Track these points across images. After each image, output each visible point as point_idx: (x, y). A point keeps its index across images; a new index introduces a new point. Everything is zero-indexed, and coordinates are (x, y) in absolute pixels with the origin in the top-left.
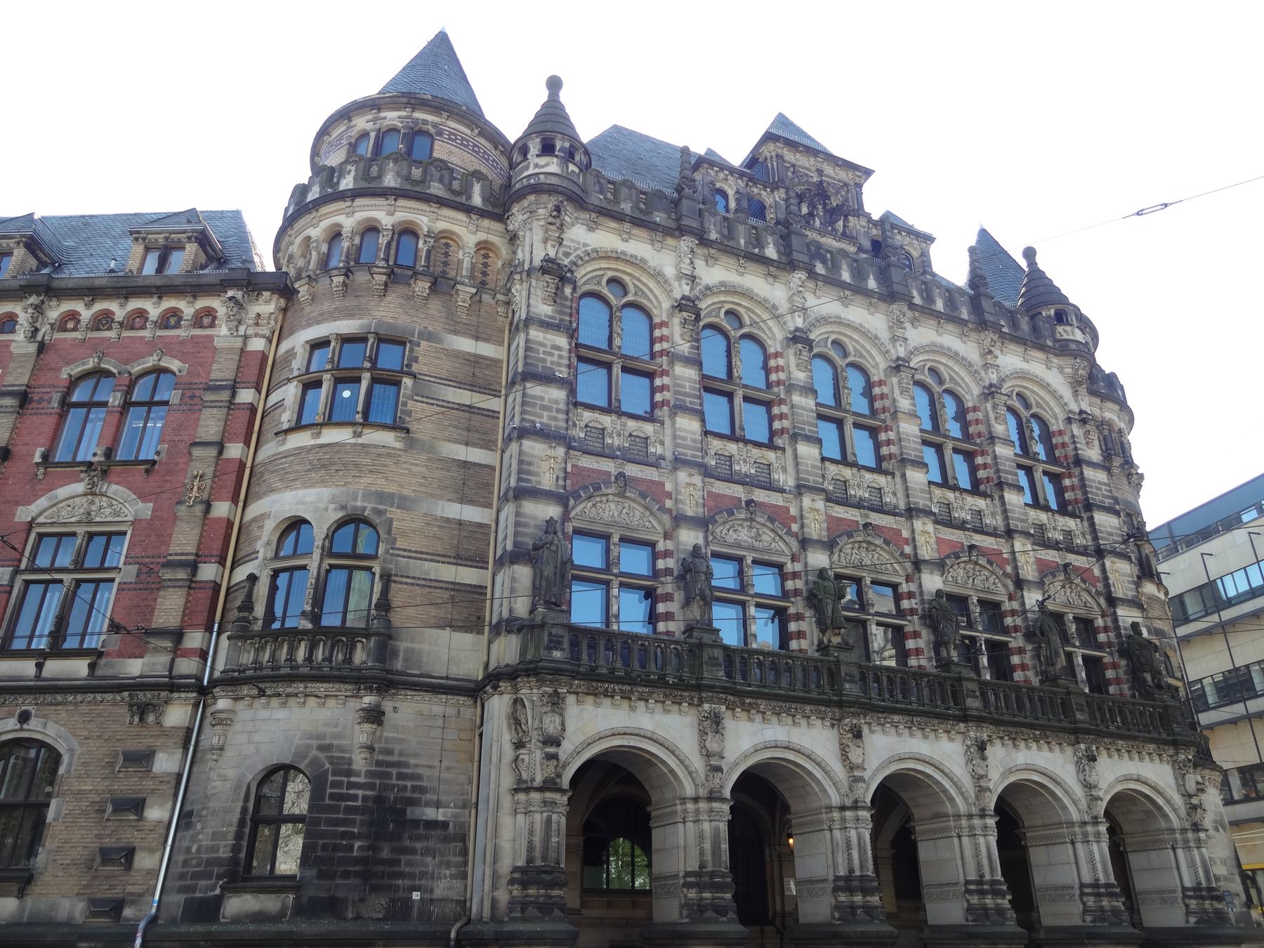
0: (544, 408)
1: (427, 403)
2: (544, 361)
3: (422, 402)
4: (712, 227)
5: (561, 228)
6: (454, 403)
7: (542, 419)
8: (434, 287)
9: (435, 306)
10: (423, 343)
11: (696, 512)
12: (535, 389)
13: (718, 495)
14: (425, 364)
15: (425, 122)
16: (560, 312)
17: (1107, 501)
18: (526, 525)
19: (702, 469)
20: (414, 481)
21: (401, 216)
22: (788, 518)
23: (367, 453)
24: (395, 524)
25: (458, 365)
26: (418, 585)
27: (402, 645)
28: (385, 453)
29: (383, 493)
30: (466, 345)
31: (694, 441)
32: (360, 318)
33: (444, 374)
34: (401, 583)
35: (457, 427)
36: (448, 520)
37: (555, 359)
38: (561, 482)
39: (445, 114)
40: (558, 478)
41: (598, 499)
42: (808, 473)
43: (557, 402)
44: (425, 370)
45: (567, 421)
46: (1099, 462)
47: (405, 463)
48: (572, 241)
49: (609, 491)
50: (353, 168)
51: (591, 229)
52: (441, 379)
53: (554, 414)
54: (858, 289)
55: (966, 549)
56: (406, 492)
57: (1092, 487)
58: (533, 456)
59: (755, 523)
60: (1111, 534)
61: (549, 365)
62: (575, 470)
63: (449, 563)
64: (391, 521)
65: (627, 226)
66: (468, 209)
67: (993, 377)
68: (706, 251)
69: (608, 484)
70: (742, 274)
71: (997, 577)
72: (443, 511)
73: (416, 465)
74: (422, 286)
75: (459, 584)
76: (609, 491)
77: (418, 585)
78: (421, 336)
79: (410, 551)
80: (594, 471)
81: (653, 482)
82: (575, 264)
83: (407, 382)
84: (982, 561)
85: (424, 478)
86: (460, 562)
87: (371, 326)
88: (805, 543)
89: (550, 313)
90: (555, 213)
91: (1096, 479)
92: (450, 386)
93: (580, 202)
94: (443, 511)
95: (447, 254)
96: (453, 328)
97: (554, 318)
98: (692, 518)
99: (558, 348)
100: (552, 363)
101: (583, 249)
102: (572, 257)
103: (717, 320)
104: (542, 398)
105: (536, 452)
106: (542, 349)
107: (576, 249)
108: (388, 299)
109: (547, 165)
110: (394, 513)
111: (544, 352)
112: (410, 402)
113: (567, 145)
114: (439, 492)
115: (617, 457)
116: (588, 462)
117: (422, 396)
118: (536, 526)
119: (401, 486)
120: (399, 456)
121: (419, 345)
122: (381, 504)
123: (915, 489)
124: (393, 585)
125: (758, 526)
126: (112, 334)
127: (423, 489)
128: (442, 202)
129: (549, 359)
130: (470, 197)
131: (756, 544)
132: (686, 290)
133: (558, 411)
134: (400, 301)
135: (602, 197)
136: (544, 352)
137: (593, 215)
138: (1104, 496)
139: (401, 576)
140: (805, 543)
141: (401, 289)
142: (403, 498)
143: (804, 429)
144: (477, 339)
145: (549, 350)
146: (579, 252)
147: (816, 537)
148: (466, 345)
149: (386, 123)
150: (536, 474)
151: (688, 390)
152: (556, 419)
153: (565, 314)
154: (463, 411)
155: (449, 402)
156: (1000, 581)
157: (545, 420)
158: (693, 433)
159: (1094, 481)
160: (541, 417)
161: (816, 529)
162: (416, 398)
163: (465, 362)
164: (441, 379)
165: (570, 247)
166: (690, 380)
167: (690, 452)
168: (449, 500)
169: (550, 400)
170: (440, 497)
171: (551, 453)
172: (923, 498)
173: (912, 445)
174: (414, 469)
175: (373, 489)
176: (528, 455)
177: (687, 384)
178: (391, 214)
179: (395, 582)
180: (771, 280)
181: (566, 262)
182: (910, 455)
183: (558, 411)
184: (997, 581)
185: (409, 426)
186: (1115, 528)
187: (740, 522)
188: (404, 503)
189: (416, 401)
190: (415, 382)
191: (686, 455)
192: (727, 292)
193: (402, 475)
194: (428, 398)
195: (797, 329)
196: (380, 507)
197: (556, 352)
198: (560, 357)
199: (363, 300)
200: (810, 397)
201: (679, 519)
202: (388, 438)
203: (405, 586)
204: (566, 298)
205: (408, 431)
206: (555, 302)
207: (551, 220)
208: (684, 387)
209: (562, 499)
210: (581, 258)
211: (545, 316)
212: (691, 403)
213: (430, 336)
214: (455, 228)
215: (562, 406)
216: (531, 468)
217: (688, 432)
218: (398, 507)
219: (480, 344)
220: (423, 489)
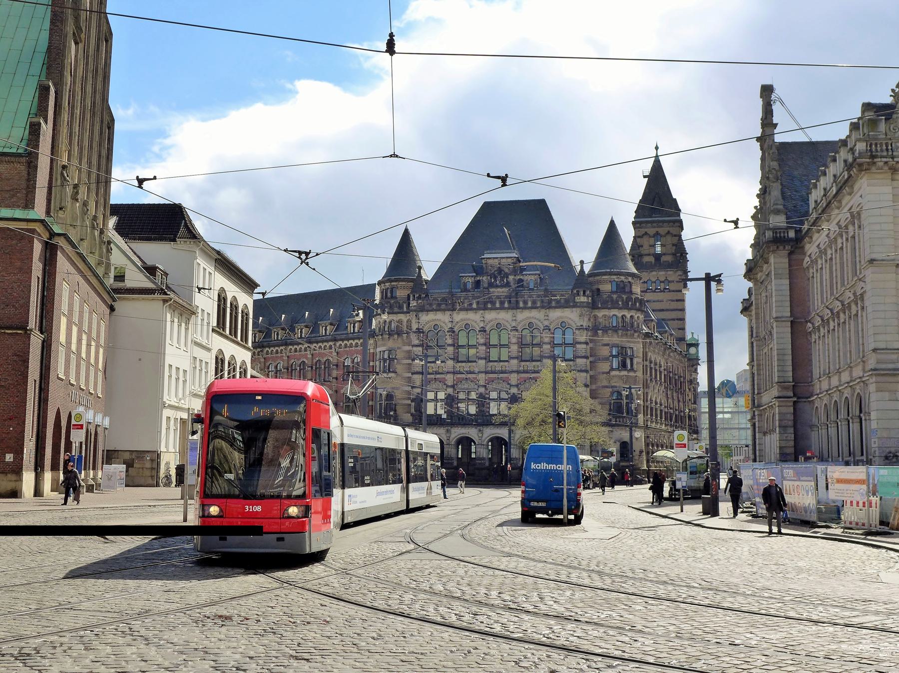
5: (419, 319)
8: (398, 335)
27: (399, 418)
54: (502, 308)
66: (403, 313)
67: (546, 323)
69: (432, 381)
74: (396, 336)
110: (395, 391)
126: (348, 349)
141: (392, 338)
148: (407, 348)
161: (482, 383)
188: (397, 389)
201: (447, 386)
202: (391, 375)
213: (399, 348)
214: (400, 318)
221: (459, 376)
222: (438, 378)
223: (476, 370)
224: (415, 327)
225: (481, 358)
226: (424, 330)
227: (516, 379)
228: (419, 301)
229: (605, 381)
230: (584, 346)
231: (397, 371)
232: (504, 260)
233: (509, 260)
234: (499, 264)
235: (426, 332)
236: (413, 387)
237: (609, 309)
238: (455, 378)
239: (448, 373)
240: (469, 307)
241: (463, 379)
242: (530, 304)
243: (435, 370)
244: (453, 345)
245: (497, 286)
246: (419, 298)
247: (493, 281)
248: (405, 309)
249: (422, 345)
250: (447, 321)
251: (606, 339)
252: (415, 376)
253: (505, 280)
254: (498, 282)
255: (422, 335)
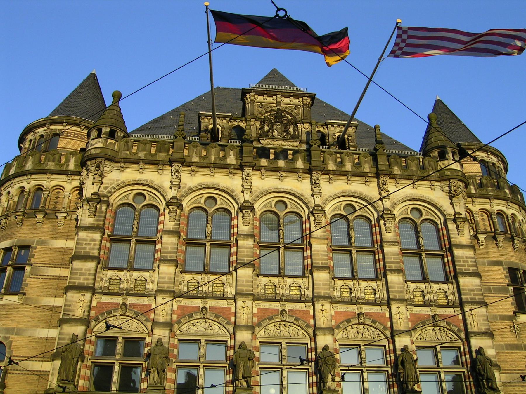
0: (81, 274)
1: (37, 278)
2: (85, 248)
3: (34, 278)
4: (194, 154)
5: (102, 176)
6: (51, 276)
7: (81, 280)
9: (47, 226)
10: (39, 247)
11: (166, 320)
12: (77, 264)
13: (185, 307)
14: (38, 258)
15: (56, 130)
16: (98, 220)
17: (471, 268)
18: (64, 339)
19: (172, 294)
20: (25, 320)
21: (34, 183)
22: (229, 314)
23: (4, 308)
24: (13, 343)
25: (55, 255)
26: (22, 374)
28: (13, 307)
29: (9, 328)
30: (61, 244)
31: (170, 278)
32: (10, 239)
33: (47, 261)
34: (13, 373)
35: (51, 288)
36: (41, 338)
37: (92, 246)
38: (86, 313)
39: (65, 124)
40: (84, 311)
41: (112, 319)
42: (243, 286)
43: (89, 270)
44: (38, 261)
45: (94, 279)
46: (468, 244)
47: (22, 311)
48: (110, 180)
49: (116, 314)
50: (16, 163)
51: (121, 171)
52: (45, 264)
53: (87, 277)
54: (291, 170)
55: (357, 316)
56: (20, 326)
57: (460, 261)
58: (72, 301)
59: (207, 320)
60: (473, 290)
61: (88, 250)
62: (98, 305)
63: (39, 361)
64: (11, 342)
65: (142, 165)
66: (65, 173)
68: (190, 168)
69: (116, 310)
70: (212, 177)
71: (380, 331)
72: (39, 334)
73: (27, 311)
74: (40, 217)
75: (43, 371)
76: (116, 314)
77: (22, 374)
78: (38, 243)
79: (20, 357)
80: (109, 304)
81: (144, 305)
82: (110, 192)
83: (28, 268)
84: (368, 322)
85: (31, 317)
86: (45, 359)
87: (14, 243)
88: (236, 327)
89: (92, 222)
90: (97, 168)
91: (464, 256)
92: (50, 267)
93: (112, 160)
94: (39, 334)
95: (58, 197)
96: (55, 236)
97: (94, 224)
98: (163, 323)
99: (94, 240)
100: (89, 249)
101: (116, 183)
102: (109, 189)
103: (200, 205)
104: (81, 269)
105: (75, 299)
106: (84, 242)
107: (112, 184)
108: (23, 227)
109: (96, 143)
110: (14, 338)
111: (86, 244)
112: (28, 279)
113: (108, 130)
114: (38, 324)
115: (123, 294)
116: (106, 299)
117: (34, 275)
118: (69, 339)
119: (19, 323)
120: (19, 308)
121: (36, 248)
122: (7, 334)
123: (320, 285)
124: (9, 375)
125: (210, 321)
127: (30, 324)
128: (53, 172)
129: (88, 247)
130: (68, 166)
131: (209, 332)
132: (174, 193)
133: (90, 274)
134: (30, 227)
135: (128, 152)
136: (86, 244)
137: (122, 164)
138: (469, 266)
139: (14, 370)
140: (236, 327)
142: (19, 330)
143: (244, 260)
144: (67, 239)
145: (89, 242)
146: (113, 185)
147: (243, 323)
148: (61, 244)
149: (39, 134)
150: (72, 311)
151: (170, 250)
152: (87, 279)
153: (100, 221)
154: (55, 279)
155: (48, 276)
156: (382, 333)
157: (81, 281)
158: (170, 274)
159: (462, 257)
160: (80, 279)
161: (242, 319)
162: (31, 276)
163: (59, 253)
164: (45, 264)
165: (108, 184)
166: (172, 244)
167: (166, 285)
168: (43, 328)
169: (86, 270)
170: (37, 327)
171: (82, 298)
172: (325, 289)
173: (320, 257)
174: (27, 313)
175: (5, 327)
176: (70, 301)
177: (170, 246)
178: (29, 183)
179: (10, 373)
180: (231, 175)
181: (105, 192)
182: (318, 263)
183: (90, 274)
184: (380, 333)
185: (26, 292)
186: (479, 286)
187: (199, 320)
188: (19, 332)
189: (31, 278)
190: (32, 268)
191: (164, 288)
192: (205, 188)
193: (20, 317)
194: (37, 275)
195: (246, 202)
196: (6, 335)
197: (92, 243)
198: (95, 245)
199: (13, 230)
200: (250, 239)
201: (155, 323)
203: (15, 375)
204: (102, 212)
205: (24, 294)
206: (95, 215)
207: (96, 172)
208: (167, 248)
209: (86, 322)
210: (114, 188)
211: (89, 224)
212: (171, 257)
213: (42, 243)
215: (93, 272)
216: (70, 308)
217: (166, 274)
218: (16, 335)
219: (68, 241)
220: (30, 324)
221: (186, 302)
222: (131, 305)
223: (230, 291)
224: (89, 190)
225: (244, 265)
226: (111, 199)
227: (328, 314)
228: (109, 141)
229: (509, 334)
230: (470, 253)
231: (27, 290)
232: (287, 100)
233: (296, 101)
234: (278, 103)
235: (115, 206)
236: (62, 322)
237: (489, 197)
238: (175, 307)
239: (160, 291)
240: (218, 162)
241: (196, 310)
242: (348, 167)
243: (124, 285)
244: (176, 233)
245: (273, 138)
246: (112, 135)
247: (266, 128)
248: (72, 166)
249: (101, 229)
250: (167, 185)
251: (494, 254)
252: (74, 296)
253: (291, 130)
254: (275, 133)
255: (104, 207)
